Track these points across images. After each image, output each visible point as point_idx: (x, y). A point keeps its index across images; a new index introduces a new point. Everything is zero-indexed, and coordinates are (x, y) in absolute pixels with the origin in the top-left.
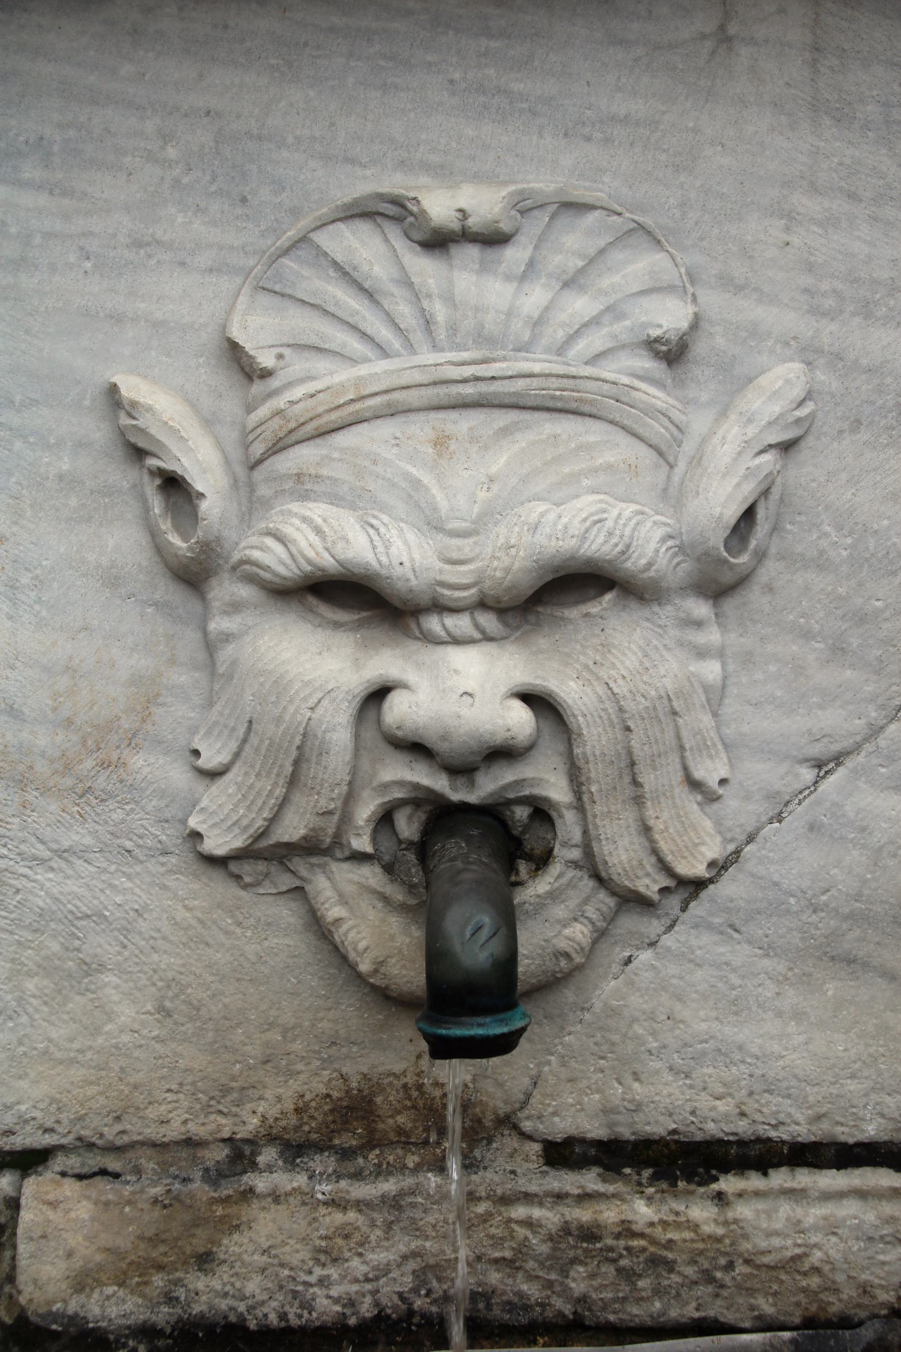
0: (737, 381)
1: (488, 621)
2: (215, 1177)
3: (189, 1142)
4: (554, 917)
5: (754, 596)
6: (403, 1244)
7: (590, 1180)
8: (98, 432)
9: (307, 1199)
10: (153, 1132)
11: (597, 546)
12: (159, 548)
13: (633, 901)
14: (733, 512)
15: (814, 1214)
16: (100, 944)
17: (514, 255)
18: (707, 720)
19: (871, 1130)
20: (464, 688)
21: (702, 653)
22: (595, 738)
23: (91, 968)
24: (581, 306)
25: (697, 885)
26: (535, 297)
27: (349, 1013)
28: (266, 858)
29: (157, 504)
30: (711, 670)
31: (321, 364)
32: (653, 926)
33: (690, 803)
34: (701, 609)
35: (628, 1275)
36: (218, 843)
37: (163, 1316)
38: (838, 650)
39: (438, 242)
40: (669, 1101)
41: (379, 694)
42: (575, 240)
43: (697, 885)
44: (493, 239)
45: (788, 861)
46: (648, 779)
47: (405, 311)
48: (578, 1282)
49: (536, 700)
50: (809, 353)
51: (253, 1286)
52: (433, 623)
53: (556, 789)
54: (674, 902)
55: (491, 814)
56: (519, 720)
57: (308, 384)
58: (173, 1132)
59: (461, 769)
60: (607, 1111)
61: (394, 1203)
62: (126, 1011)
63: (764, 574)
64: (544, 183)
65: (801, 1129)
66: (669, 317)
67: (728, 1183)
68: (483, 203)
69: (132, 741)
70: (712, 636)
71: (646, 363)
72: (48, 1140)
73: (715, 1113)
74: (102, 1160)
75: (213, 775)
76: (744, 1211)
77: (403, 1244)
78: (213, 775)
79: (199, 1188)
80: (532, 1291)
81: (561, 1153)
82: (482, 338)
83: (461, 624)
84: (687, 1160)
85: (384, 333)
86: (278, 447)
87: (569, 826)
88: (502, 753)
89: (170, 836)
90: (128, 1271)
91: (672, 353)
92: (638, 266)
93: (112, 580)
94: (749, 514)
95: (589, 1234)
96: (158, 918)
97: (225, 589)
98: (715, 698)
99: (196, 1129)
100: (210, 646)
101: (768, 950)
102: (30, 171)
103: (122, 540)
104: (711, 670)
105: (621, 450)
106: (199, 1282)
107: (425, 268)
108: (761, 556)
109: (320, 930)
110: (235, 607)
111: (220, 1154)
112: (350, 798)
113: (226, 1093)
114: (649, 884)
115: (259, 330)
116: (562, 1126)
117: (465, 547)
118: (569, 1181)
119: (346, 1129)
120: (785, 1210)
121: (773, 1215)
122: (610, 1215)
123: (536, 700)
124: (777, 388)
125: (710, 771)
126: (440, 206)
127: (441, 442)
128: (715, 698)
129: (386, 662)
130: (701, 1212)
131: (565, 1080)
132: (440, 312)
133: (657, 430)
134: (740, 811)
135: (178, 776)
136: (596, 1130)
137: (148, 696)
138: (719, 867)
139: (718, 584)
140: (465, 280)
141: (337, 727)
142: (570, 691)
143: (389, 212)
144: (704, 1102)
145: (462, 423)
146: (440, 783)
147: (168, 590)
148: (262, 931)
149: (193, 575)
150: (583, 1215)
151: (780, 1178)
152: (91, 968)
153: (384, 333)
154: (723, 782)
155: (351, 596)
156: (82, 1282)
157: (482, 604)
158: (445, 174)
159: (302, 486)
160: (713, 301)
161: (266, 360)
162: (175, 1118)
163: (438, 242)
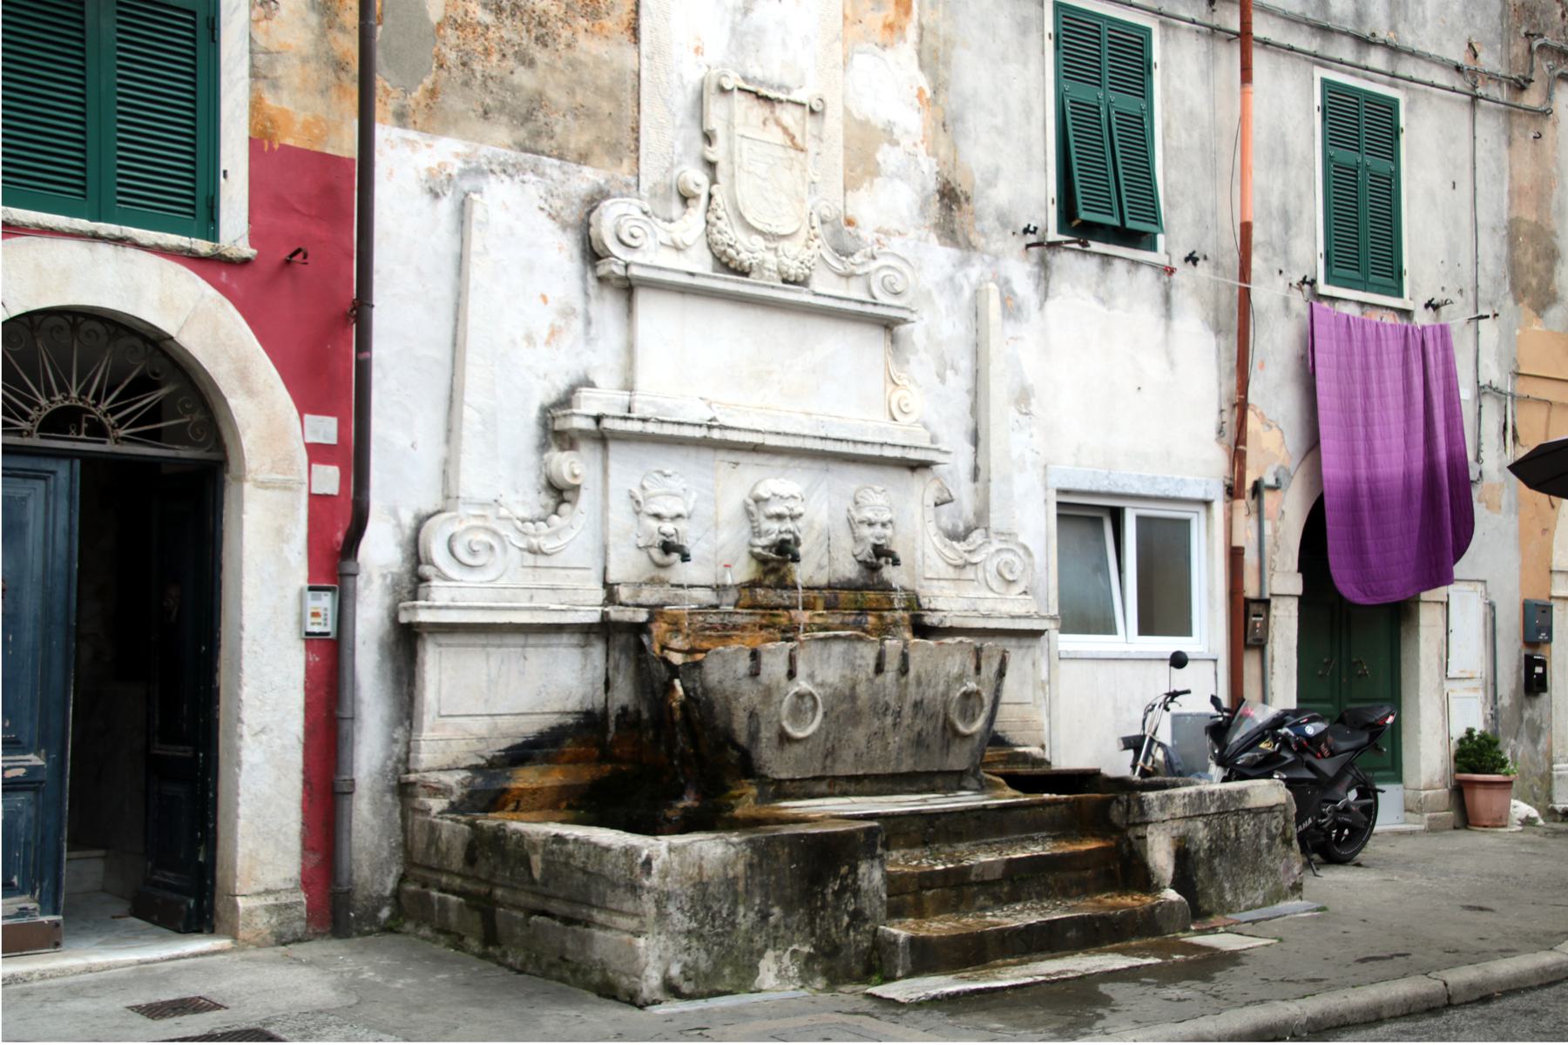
20: (668, 527)
27: (652, 567)
28: (647, 547)
40: (685, 581)
57: (652, 491)
74: (627, 584)
96: (633, 552)
103: (630, 509)
109: (651, 557)
115: (646, 484)
119: (652, 582)
124: (694, 495)
140: (668, 480)
143: (660, 472)
148: (644, 557)
149: (637, 513)
155: (658, 516)
162: (634, 579)
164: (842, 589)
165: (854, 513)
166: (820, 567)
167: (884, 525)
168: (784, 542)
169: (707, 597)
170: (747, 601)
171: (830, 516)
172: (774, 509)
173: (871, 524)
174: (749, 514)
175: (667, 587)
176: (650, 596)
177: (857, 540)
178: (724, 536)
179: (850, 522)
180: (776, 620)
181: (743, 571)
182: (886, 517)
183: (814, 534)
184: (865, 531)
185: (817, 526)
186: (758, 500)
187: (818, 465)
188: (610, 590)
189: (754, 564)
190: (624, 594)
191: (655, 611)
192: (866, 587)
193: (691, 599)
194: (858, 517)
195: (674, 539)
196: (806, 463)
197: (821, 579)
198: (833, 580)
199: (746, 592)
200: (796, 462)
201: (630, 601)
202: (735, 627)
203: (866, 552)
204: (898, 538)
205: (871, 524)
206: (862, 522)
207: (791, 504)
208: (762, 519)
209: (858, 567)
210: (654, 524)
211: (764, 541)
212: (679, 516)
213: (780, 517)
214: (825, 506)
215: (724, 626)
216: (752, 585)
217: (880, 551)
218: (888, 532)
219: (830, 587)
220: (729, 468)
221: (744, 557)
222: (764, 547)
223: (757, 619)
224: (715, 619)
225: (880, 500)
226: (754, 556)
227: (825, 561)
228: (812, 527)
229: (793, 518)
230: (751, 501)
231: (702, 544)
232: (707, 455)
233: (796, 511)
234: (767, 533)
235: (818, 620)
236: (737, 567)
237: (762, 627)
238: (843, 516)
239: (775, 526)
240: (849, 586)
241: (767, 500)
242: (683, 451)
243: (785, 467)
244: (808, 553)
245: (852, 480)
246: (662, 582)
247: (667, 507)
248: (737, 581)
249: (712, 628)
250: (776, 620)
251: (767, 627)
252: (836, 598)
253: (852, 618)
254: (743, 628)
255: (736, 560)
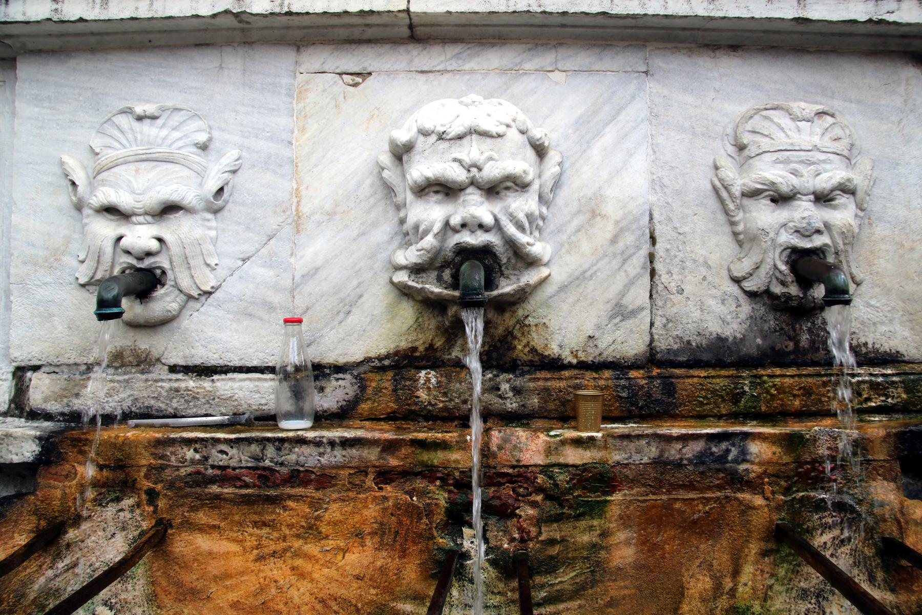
0: (221, 154)
1: (149, 218)
2: (82, 374)
3: (76, 364)
4: (164, 301)
5: (225, 213)
6: (128, 392)
7: (180, 376)
8: (58, 170)
9: (104, 380)
10: (66, 361)
11: (175, 198)
12: (71, 200)
13: (190, 297)
14: (215, 189)
15: (236, 385)
16: (54, 309)
17: (159, 122)
18: (211, 247)
19: (255, 363)
20: (141, 236)
21: (210, 228)
22: (175, 249)
23: (51, 315)
24: (176, 135)
25: (210, 293)
26: (164, 132)
29: (70, 188)
30: (213, 233)
31: (110, 151)
32: (197, 305)
33: (207, 271)
34: (209, 216)
35: (187, 402)
36: (83, 280)
37: (66, 410)
38: (248, 228)
39: (140, 119)
41: (120, 238)
42: (177, 118)
43: (210, 293)
44: (154, 118)
45: (233, 288)
46: (192, 262)
47: (130, 136)
48: (175, 404)
49: (160, 240)
50: (241, 147)
51: (89, 403)
52: (134, 219)
53: (166, 265)
54: (203, 298)
55: (149, 271)
56: (154, 245)
58: (71, 361)
59: (140, 259)
60: (185, 357)
61: (127, 381)
62: (60, 327)
63: (228, 207)
64: (170, 104)
65: (237, 363)
66: (202, 138)
67: (216, 377)
68: (150, 109)
69: (63, 253)
70: (213, 224)
71: (195, 150)
72: (39, 363)
73: (213, 359)
74: (54, 368)
75: (82, 262)
76: (218, 384)
77: (128, 392)
78: (82, 262)
79: (78, 377)
80: (163, 406)
81: (173, 369)
82: (149, 143)
83: (141, 219)
84: (205, 371)
85: (125, 142)
86: (99, 173)
87: (170, 274)
88: (149, 254)
89: (72, 279)
90: (58, 398)
91: (204, 147)
92: (195, 124)
93: (60, 210)
94: (221, 190)
95: (177, 390)
97: (87, 211)
98: (214, 241)
99: (78, 361)
100: (84, 226)
101: (228, 312)
102: (46, 104)
103: (64, 199)
104: (213, 233)
105: (186, 172)
106: (76, 401)
107: (137, 125)
108: (227, 202)
110: (88, 216)
111: (84, 368)
112: (112, 267)
113: (86, 351)
114: (195, 293)
115: (97, 143)
116: (173, 361)
117: (140, 198)
118: (174, 376)
120: (230, 383)
121: (224, 385)
122: (183, 385)
123: (160, 240)
124: (229, 158)
125: (212, 261)
126: (139, 110)
127: (137, 171)
128: (214, 241)
129: (123, 229)
130: (206, 384)
131: (173, 348)
132: (139, 137)
133: (196, 167)
134: (221, 272)
135: (75, 263)
136: (182, 362)
137: (68, 241)
138: (215, 289)
139: (216, 211)
140: (146, 128)
141: (108, 248)
142: (167, 237)
143: (128, 111)
144: (210, 355)
145: (143, 165)
146: (134, 262)
147: (74, 212)
150: (176, 385)
151: (230, 375)
152: (51, 315)
153: (125, 142)
154: (216, 265)
155: (111, 210)
156: (46, 400)
157: (146, 213)
158: (140, 101)
159: (103, 183)
160: (215, 134)
161: (97, 150)
162: (73, 357)
163: (140, 119)
164: (695, 363)
165: (730, 172)
166: (621, 312)
167: (822, 198)
168: (465, 253)
169: (259, 393)
170: (388, 404)
171: (656, 184)
172: (423, 168)
173: (781, 199)
174: (389, 190)
175: (161, 372)
176: (98, 394)
177: (743, 240)
178: (316, 247)
179: (721, 191)
180: (438, 458)
181: (371, 328)
182: (831, 175)
183: (603, 231)
184: (764, 216)
185: (612, 210)
186: (401, 153)
187: (633, 60)
188: (20, 373)
189: (407, 312)
190: (41, 391)
191: (66, 436)
192: (774, 357)
193: (211, 398)
194: (739, 182)
195: (162, 261)
196: (581, 59)
197: (629, 342)
198: (662, 345)
199: (386, 381)
200: (546, 59)
201: (53, 407)
202: (298, 477)
203: (769, 267)
204: (880, 230)
205: (781, 199)
206: (753, 194)
207: (473, 151)
208: (410, 197)
209: (746, 308)
210: (105, 230)
211: (410, 256)
212: (169, 209)
213: (446, 190)
214: (640, 163)
215: (265, 476)
216: (402, 363)
217: (808, 264)
218: (843, 215)
219: (652, 359)
220: (339, 86)
221: (377, 297)
222: (417, 270)
223: (372, 455)
224: (238, 457)
225: (809, 136)
226: (404, 292)
227: (639, 295)
228: (594, 214)
229: (493, 190)
230: (386, 159)
231: (258, 271)
232: (277, 66)
233: (492, 172)
234: (418, 232)
235: (573, 456)
236: (355, 318)
237: (385, 476)
238: (703, 181)
239: (432, 213)
240: (716, 355)
241: (408, 148)
242: (207, 61)
243: (516, 72)
244: (580, 278)
245: (728, 93)
246: (144, 362)
247: (135, 188)
248: (355, 352)
249: (226, 476)
250: (438, 458)
251: (405, 474)
252: (669, 388)
253: (696, 447)
254: (324, 479)
255: (347, 307)
